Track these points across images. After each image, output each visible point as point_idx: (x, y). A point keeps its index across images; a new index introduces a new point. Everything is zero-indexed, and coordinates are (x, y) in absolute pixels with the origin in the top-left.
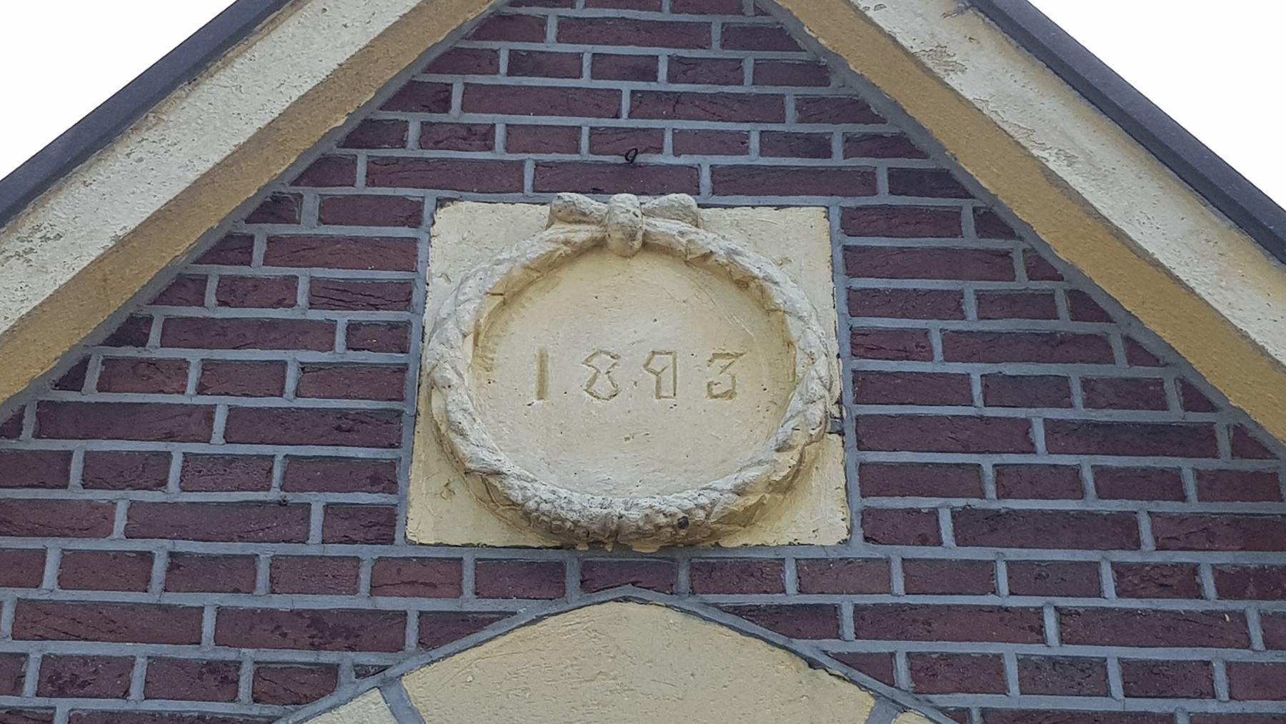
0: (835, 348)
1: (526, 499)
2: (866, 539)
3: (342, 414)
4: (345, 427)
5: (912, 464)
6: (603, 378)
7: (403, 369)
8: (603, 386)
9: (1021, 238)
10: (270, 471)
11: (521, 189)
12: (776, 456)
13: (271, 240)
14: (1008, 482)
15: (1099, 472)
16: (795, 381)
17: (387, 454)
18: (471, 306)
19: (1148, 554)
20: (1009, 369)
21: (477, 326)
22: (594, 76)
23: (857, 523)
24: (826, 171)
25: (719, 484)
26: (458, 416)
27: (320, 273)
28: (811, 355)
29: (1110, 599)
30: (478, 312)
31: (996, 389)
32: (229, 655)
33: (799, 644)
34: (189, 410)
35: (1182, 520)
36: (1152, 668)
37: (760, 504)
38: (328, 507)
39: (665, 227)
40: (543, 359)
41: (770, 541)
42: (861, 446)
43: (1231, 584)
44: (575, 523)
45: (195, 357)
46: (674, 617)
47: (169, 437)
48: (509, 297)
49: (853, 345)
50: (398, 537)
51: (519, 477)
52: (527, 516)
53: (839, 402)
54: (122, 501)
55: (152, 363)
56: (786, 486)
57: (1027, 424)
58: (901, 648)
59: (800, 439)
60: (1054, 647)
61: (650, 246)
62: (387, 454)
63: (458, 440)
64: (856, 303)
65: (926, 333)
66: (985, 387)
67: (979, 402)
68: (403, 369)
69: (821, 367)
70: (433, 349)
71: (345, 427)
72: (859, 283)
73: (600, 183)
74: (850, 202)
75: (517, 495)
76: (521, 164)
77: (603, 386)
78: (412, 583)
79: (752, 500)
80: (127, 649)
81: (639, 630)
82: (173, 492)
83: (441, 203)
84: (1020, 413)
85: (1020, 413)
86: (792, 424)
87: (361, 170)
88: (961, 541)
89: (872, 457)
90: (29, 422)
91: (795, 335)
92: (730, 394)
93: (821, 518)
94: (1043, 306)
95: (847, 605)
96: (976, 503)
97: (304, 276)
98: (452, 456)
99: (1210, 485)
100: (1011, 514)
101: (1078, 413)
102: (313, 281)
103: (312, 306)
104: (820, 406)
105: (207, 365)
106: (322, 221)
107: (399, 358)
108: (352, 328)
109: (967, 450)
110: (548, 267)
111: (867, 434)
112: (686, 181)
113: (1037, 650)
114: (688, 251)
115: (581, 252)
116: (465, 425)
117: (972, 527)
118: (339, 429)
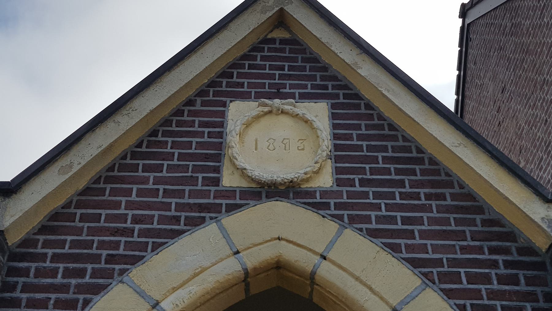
0: (329, 138)
1: (252, 175)
2: (337, 185)
3: (207, 154)
4: (207, 157)
5: (349, 167)
6: (271, 145)
7: (222, 143)
8: (271, 147)
9: (376, 110)
10: (189, 168)
11: (251, 98)
12: (315, 165)
13: (189, 111)
14: (373, 171)
15: (395, 169)
16: (319, 146)
17: (218, 164)
18: (238, 127)
19: (408, 189)
20: (373, 143)
21: (240, 132)
22: (269, 70)
23: (335, 181)
24: (327, 93)
25: (301, 172)
26: (235, 155)
27: (201, 119)
28: (323, 140)
29: (398, 201)
30: (240, 129)
31: (370, 148)
32: (178, 214)
33: (320, 212)
34: (169, 153)
35: (416, 181)
36: (409, 218)
37: (310, 177)
38: (203, 177)
39: (287, 108)
40: (256, 140)
41: (313, 186)
42: (336, 162)
44: (265, 181)
45: (170, 140)
46: (289, 205)
47: (163, 160)
48: (248, 125)
49: (334, 137)
50: (220, 185)
51: (250, 170)
52: (253, 180)
53: (330, 151)
54: (152, 175)
55: (159, 141)
56: (317, 172)
57: (377, 157)
58: (346, 213)
59: (320, 161)
60: (384, 212)
61: (283, 112)
62: (218, 164)
63: (235, 161)
64: (335, 126)
65: (352, 134)
66: (367, 147)
67: (365, 151)
68: (222, 143)
69: (326, 142)
70: (229, 138)
71: (207, 157)
72: (336, 122)
73: (270, 97)
74: (333, 101)
75: (250, 175)
76: (251, 92)
77: (271, 147)
78: (224, 196)
79: (309, 176)
80: (153, 212)
81: (280, 207)
82: (164, 174)
83: (231, 101)
84: (376, 154)
85: (376, 154)
86: (318, 157)
87: (211, 93)
88: (361, 186)
89: (338, 165)
90: (129, 156)
91: (319, 134)
92: (303, 149)
93: (326, 180)
94: (382, 127)
95: (332, 202)
96: (364, 177)
97: (197, 120)
98: (234, 165)
99: (424, 172)
100: (374, 179)
101: (390, 154)
102: (199, 121)
103: (199, 127)
104: (326, 152)
105: (173, 142)
106: (202, 106)
107: (221, 140)
108: (209, 133)
109: (362, 163)
110: (258, 118)
111: (338, 159)
113: (379, 213)
114: (293, 114)
115: (266, 114)
116: (237, 157)
117: (363, 183)
118: (206, 158)
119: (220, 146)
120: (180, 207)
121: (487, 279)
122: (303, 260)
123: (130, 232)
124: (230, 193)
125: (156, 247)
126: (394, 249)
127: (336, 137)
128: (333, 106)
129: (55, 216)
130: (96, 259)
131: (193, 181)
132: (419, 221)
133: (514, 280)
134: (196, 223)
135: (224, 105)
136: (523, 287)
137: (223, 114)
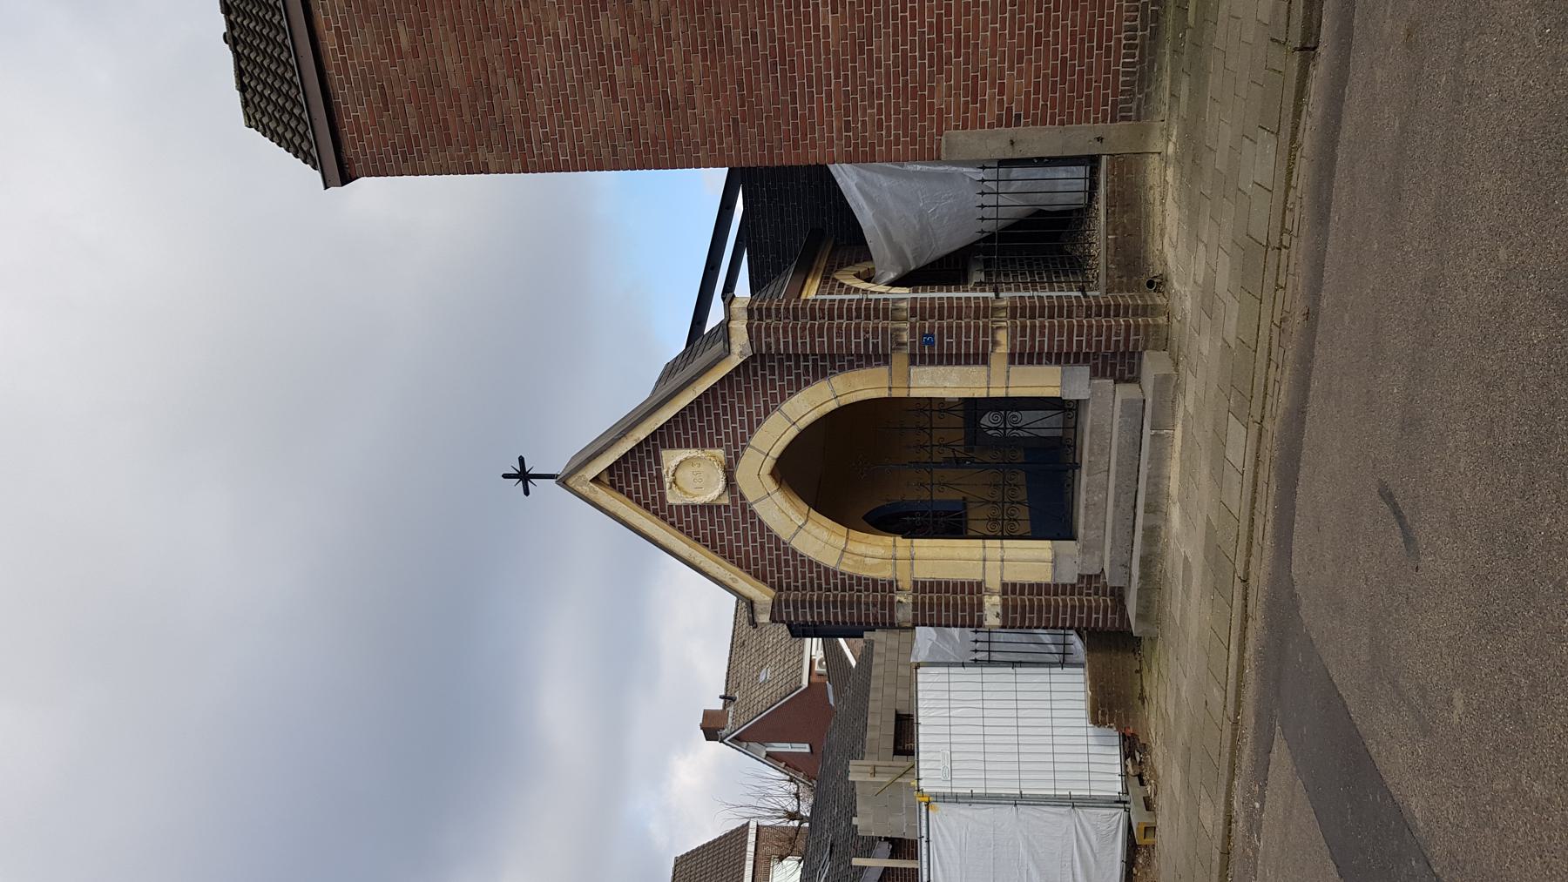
4: (711, 512)
71: (711, 512)
93: (720, 453)
117: (719, 433)
122: (769, 464)
123: (762, 544)
124: (734, 500)
126: (759, 422)
127: (687, 446)
128: (664, 447)
129: (756, 577)
130: (778, 556)
133: (772, 369)
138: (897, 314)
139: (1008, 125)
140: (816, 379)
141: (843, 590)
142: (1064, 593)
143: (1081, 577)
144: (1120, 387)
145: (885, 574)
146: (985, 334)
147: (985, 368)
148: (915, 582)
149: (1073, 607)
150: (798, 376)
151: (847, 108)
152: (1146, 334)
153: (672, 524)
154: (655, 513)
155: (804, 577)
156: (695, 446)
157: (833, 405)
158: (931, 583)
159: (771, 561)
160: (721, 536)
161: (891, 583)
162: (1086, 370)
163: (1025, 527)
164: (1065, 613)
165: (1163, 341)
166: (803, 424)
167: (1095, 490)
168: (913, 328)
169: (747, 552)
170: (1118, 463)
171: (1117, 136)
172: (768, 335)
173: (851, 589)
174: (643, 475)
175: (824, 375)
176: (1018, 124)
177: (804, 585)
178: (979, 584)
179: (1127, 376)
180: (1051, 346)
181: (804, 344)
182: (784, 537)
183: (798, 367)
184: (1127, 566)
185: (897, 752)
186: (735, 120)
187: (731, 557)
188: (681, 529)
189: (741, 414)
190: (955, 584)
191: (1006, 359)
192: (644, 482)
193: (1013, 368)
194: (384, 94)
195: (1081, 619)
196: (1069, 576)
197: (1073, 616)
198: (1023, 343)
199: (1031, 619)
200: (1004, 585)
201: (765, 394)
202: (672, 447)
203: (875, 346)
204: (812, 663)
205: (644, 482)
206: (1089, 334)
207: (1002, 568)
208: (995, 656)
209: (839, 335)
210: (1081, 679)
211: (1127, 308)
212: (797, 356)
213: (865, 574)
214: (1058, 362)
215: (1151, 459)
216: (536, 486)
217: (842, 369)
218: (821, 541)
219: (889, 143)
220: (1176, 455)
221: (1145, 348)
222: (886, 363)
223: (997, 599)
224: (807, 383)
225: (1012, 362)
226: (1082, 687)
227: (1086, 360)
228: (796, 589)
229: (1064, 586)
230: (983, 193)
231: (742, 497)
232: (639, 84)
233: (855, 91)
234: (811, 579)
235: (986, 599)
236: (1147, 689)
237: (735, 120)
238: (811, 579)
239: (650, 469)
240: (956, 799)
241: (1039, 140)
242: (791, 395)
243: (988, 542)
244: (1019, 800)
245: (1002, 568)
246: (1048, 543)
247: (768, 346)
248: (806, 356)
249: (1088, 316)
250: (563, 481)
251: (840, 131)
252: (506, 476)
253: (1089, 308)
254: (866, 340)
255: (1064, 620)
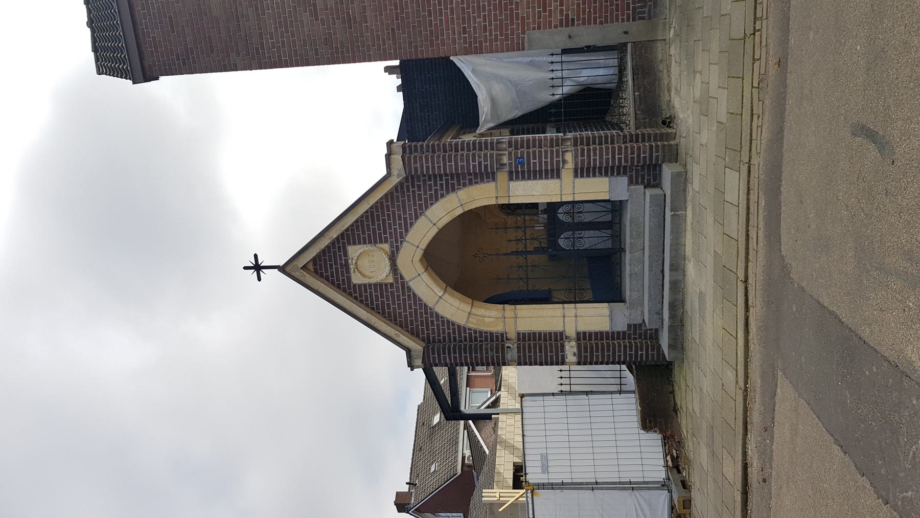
14: (379, 229)
43: (388, 211)
93: (386, 246)
111: (376, 242)
112: (346, 261)
117: (385, 233)
119: (375, 285)
120: (404, 295)
121: (420, 195)
122: (419, 253)
123: (416, 310)
124: (396, 280)
125: (420, 300)
126: (412, 224)
127: (365, 243)
128: (349, 244)
129: (412, 334)
131: (392, 293)
132: (399, 216)
133: (419, 186)
134: (409, 289)
135: (355, 285)
136: (421, 183)
137: (360, 286)
138: (500, 146)
139: (567, 26)
140: (448, 193)
141: (471, 341)
142: (618, 338)
143: (629, 326)
144: (649, 192)
145: (498, 328)
146: (558, 156)
147: (557, 181)
148: (518, 334)
149: (625, 347)
150: (436, 191)
151: (464, 18)
152: (663, 151)
153: (356, 298)
154: (344, 290)
155: (444, 333)
156: (370, 243)
157: (460, 211)
158: (529, 334)
159: (422, 322)
160: (388, 305)
161: (502, 335)
162: (625, 180)
163: (589, 295)
164: (620, 351)
165: (673, 155)
166: (441, 224)
167: (635, 267)
168: (510, 154)
169: (406, 316)
170: (650, 240)
171: (637, 30)
172: (415, 162)
173: (476, 340)
174: (336, 263)
175: (453, 190)
176: (573, 25)
177: (444, 338)
178: (561, 333)
179: (652, 183)
180: (601, 163)
181: (439, 167)
182: (430, 305)
183: (436, 185)
184: (660, 313)
185: (514, 488)
186: (393, 30)
187: (395, 319)
188: (361, 301)
189: (400, 219)
190: (545, 334)
191: (572, 173)
192: (337, 269)
193: (577, 180)
194: (171, 21)
195: (631, 355)
196: (621, 326)
197: (625, 353)
198: (583, 161)
199: (597, 357)
200: (578, 334)
201: (415, 204)
202: (354, 244)
203: (486, 166)
204: (463, 458)
205: (337, 269)
206: (626, 152)
207: (576, 322)
208: (574, 388)
209: (462, 160)
210: (634, 401)
211: (649, 135)
212: (435, 176)
213: (484, 328)
214: (606, 175)
215: (672, 232)
216: (265, 274)
217: (465, 185)
218: (454, 309)
219: (491, 40)
220: (689, 228)
221: (663, 162)
222: (494, 180)
223: (574, 343)
224: (442, 196)
225: (576, 176)
226: (634, 407)
227: (625, 173)
228: (439, 341)
229: (618, 333)
230: (552, 55)
231: (402, 278)
232: (331, 8)
233: (468, 8)
234: (449, 333)
235: (566, 343)
236: (678, 403)
237: (393, 30)
238: (449, 333)
239: (341, 260)
240: (551, 486)
241: (588, 35)
242: (432, 204)
243: (566, 305)
244: (594, 486)
245: (576, 322)
246: (606, 305)
247: (416, 169)
248: (441, 176)
249: (625, 142)
250: (282, 269)
251: (459, 34)
252: (246, 268)
253: (625, 137)
254: (480, 163)
255: (619, 356)
